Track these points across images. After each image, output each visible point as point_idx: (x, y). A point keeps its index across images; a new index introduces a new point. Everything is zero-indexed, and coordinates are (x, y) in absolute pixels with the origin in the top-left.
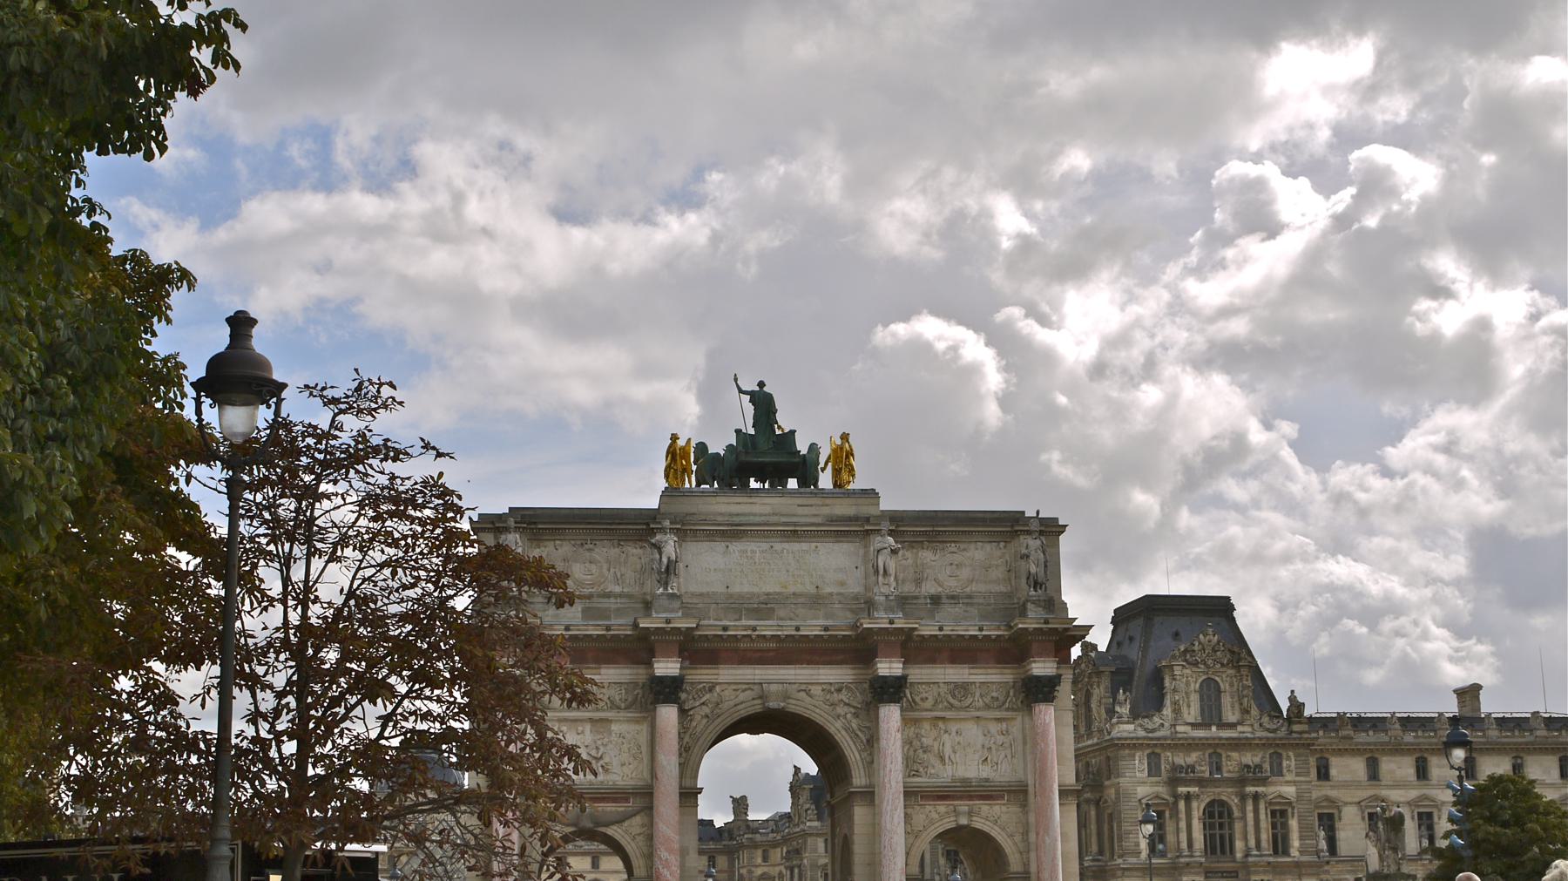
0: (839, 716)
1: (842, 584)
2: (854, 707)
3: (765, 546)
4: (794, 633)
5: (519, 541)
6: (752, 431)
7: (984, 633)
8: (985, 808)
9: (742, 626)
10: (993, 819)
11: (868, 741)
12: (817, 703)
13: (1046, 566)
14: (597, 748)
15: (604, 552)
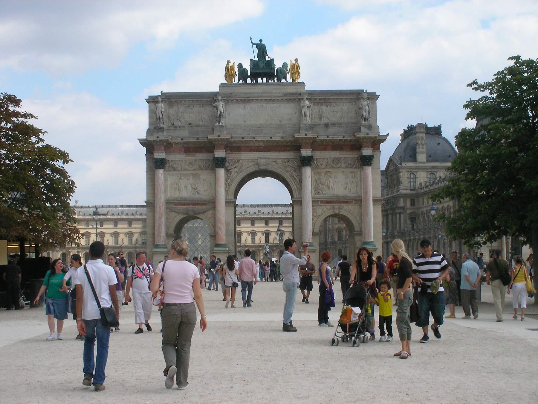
0: (288, 172)
1: (290, 120)
2: (294, 168)
5: (163, 106)
6: (257, 59)
7: (345, 138)
8: (346, 206)
9: (250, 137)
10: (348, 210)
11: (299, 181)
13: (369, 112)
14: (195, 185)
15: (196, 109)
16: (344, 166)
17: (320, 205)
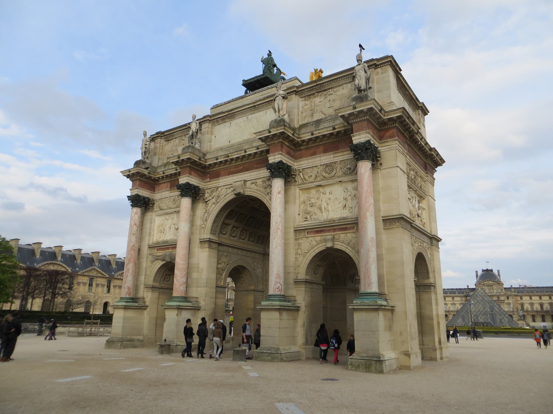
0: (268, 194)
3: (245, 118)
4: (244, 154)
8: (342, 236)
12: (259, 188)
16: (340, 173)
17: (307, 236)
